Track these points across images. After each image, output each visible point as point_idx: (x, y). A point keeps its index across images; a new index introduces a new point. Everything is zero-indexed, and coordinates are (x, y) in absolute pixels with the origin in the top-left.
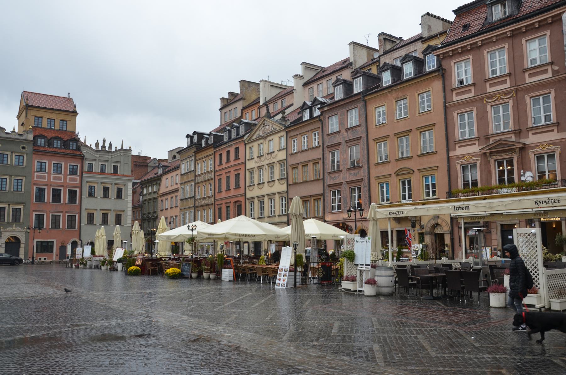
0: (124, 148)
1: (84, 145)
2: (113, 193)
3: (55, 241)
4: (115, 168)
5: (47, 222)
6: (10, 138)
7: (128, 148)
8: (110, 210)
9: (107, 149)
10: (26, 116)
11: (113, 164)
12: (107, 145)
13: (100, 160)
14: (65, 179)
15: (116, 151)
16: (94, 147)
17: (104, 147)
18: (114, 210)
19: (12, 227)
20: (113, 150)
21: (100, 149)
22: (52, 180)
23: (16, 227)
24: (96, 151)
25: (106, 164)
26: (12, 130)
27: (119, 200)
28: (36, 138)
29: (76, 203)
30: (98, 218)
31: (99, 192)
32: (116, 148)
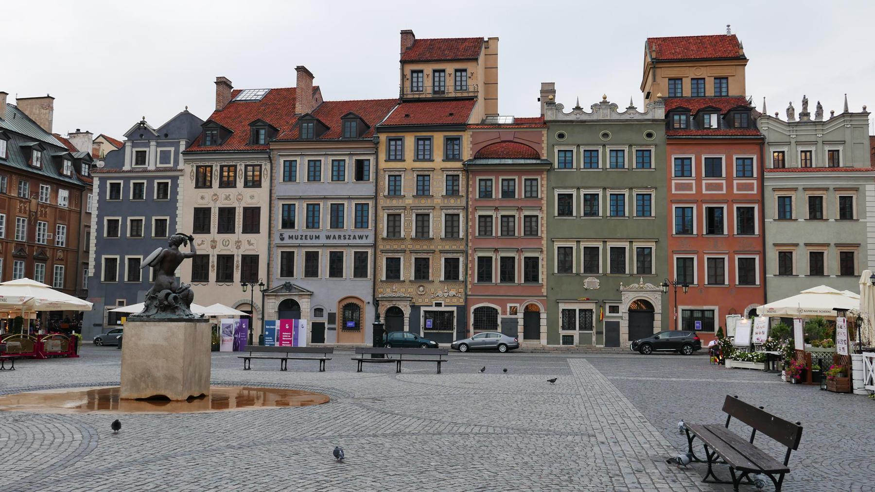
0: (851, 110)
1: (764, 116)
2: (831, 207)
3: (716, 309)
4: (834, 156)
5: (700, 273)
6: (627, 120)
7: (861, 111)
8: (828, 245)
9: (813, 118)
10: (654, 80)
11: (827, 148)
12: (812, 109)
13: (798, 143)
14: (730, 186)
15: (833, 119)
16: (784, 117)
17: (804, 114)
18: (837, 245)
19: (638, 283)
20: (826, 117)
21: (797, 119)
22: (704, 192)
23: (644, 283)
24: (789, 124)
25: (813, 149)
26: (628, 105)
27: (847, 224)
28: (671, 114)
29: (753, 233)
30: (801, 262)
31: (800, 207)
32: (832, 113)
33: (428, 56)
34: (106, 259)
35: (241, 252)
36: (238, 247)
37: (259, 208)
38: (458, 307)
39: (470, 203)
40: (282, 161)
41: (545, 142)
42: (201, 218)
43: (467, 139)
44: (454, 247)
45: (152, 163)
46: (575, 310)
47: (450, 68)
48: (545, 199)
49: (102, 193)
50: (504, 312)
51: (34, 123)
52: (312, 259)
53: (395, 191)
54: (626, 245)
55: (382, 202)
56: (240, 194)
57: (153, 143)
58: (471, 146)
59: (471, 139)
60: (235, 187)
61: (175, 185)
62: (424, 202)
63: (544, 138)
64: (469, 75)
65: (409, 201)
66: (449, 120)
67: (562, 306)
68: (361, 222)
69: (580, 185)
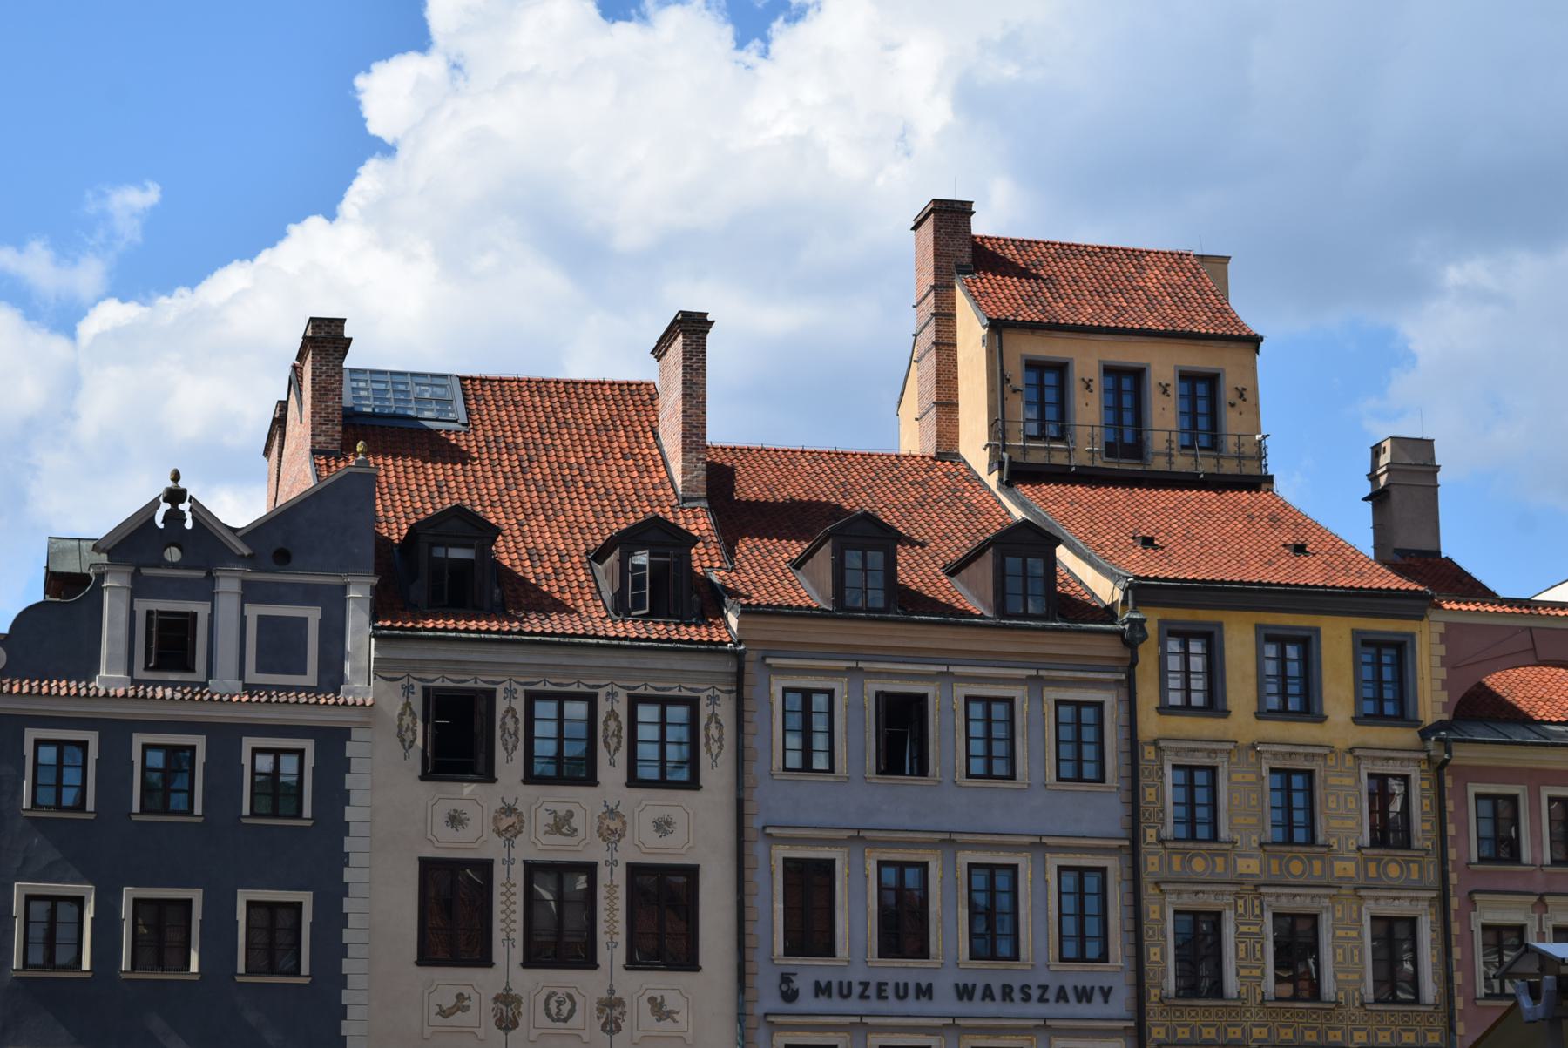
37: (691, 873)
39: (1453, 878)
40: (777, 685)
56: (612, 813)
57: (228, 585)
59: (1441, 650)
60: (591, 780)
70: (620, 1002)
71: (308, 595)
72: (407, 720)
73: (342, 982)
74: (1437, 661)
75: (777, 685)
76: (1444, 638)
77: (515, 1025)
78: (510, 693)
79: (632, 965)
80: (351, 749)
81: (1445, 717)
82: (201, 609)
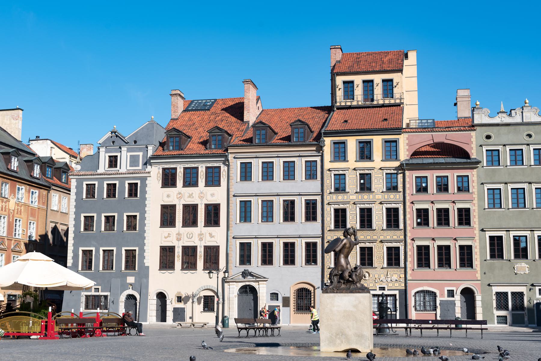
33: (356, 68)
34: (84, 251)
35: (204, 244)
36: (201, 240)
38: (400, 290)
41: (474, 143)
42: (168, 216)
43: (403, 140)
44: (395, 237)
45: (124, 166)
46: (506, 294)
47: (378, 79)
48: (476, 193)
49: (79, 193)
50: (442, 295)
51: (5, 131)
52: (267, 249)
53: (340, 189)
54: (527, 233)
55: (328, 198)
56: (202, 193)
57: (124, 149)
58: (407, 147)
59: (407, 142)
61: (144, 185)
62: (366, 196)
63: (473, 139)
64: (395, 84)
65: (354, 197)
66: (385, 125)
67: (496, 289)
68: (311, 215)
69: (507, 181)
70: (203, 234)
71: (140, 150)
72: (159, 175)
73: (145, 232)
74: (406, 145)
75: (239, 162)
76: (407, 139)
77: (180, 240)
78: (180, 168)
79: (205, 226)
80: (147, 182)
81: (408, 158)
82: (118, 154)
